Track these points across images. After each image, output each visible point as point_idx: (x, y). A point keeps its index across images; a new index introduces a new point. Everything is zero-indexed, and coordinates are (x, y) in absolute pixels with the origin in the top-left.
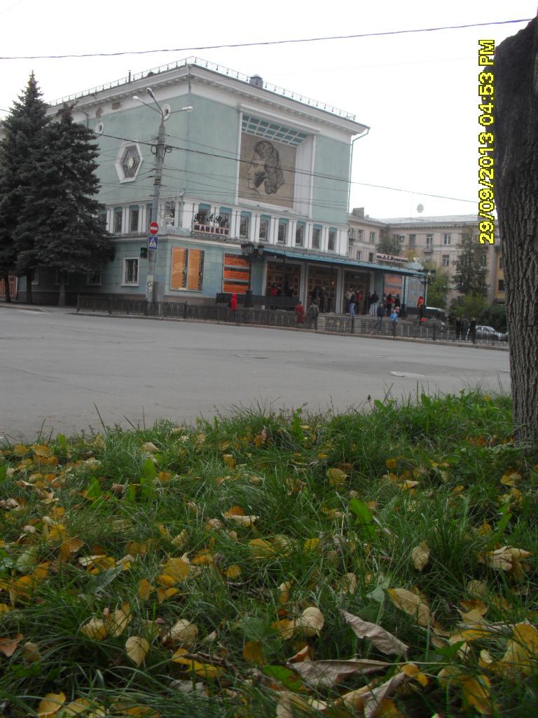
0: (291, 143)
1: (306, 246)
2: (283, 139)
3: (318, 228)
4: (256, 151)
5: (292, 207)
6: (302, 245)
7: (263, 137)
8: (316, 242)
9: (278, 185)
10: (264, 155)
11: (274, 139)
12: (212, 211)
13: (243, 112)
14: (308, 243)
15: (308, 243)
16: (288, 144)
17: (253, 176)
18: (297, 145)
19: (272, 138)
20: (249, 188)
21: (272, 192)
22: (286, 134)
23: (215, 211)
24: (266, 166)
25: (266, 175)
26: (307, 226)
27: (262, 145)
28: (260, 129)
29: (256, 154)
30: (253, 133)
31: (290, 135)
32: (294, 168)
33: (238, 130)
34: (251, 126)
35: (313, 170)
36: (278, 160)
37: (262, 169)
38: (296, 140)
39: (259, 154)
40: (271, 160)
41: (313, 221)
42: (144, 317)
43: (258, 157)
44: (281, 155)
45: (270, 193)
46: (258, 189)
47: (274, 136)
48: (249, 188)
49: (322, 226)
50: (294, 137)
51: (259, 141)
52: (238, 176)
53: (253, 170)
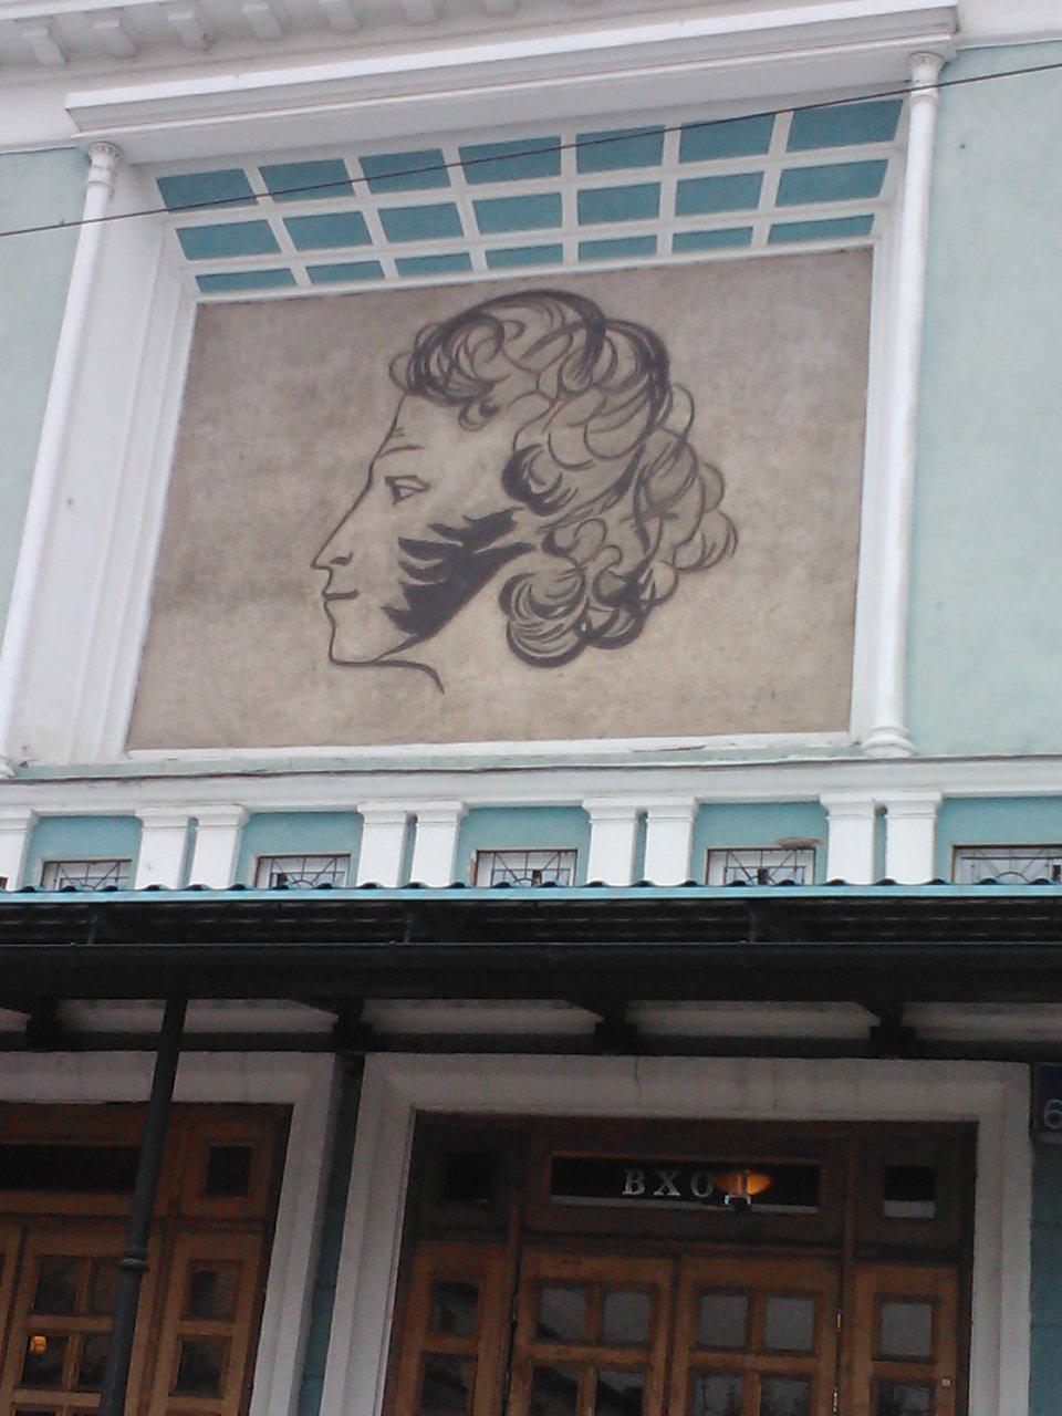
0: (779, 233)
2: (666, 225)
4: (421, 384)
7: (481, 272)
9: (661, 575)
10: (499, 395)
11: (589, 250)
13: (115, 149)
16: (759, 248)
18: (863, 224)
27: (478, 335)
29: (420, 402)
37: (488, 496)
39: (452, 401)
40: (591, 399)
43: (435, 424)
46: (427, 652)
47: (570, 233)
51: (446, 313)
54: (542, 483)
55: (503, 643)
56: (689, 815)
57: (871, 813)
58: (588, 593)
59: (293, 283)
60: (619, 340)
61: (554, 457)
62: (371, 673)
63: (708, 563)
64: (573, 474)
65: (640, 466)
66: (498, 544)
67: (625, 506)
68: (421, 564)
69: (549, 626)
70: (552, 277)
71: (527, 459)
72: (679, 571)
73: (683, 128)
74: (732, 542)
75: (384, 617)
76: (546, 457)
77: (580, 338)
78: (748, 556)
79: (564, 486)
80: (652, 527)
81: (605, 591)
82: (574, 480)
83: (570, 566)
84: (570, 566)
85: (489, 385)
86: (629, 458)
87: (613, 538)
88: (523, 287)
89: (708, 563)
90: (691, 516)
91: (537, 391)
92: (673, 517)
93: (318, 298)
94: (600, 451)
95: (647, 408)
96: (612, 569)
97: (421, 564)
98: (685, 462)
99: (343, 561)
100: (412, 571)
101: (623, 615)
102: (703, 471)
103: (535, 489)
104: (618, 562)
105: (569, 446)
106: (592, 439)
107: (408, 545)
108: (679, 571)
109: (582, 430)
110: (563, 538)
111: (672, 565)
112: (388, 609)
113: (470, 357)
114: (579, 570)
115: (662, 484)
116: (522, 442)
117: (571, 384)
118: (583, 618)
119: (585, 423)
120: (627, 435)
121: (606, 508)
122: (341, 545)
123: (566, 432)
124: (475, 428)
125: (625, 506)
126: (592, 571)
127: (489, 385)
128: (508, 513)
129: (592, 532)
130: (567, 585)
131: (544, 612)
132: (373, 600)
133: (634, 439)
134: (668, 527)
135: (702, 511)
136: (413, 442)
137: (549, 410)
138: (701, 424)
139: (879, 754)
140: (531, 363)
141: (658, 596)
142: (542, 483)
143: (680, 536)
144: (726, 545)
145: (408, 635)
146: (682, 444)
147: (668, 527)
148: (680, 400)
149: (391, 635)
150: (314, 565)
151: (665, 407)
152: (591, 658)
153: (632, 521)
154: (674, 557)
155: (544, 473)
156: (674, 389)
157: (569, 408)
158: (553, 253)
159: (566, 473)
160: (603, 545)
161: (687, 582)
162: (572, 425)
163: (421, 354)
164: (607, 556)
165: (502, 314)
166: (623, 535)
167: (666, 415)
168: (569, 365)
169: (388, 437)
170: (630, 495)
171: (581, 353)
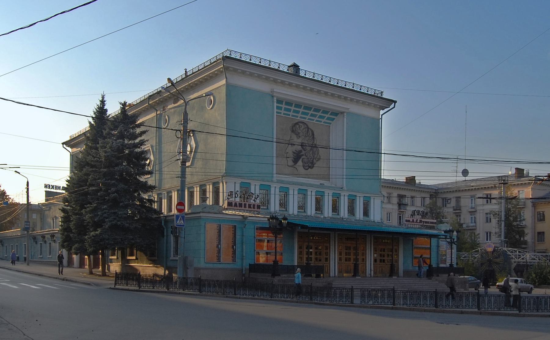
1: (342, 215)
2: (316, 119)
3: (353, 198)
4: (293, 131)
5: (327, 177)
6: (338, 214)
8: (352, 210)
9: (315, 161)
10: (301, 135)
11: (309, 119)
12: (253, 188)
14: (344, 212)
15: (344, 212)
16: (322, 123)
17: (291, 154)
19: (307, 119)
20: (288, 165)
21: (310, 167)
22: (319, 114)
23: (255, 189)
24: (302, 145)
25: (303, 152)
26: (342, 198)
27: (298, 126)
28: (295, 111)
29: (292, 133)
30: (289, 115)
31: (322, 115)
32: (330, 146)
33: (273, 113)
34: (286, 109)
35: (345, 145)
36: (313, 138)
37: (299, 148)
38: (328, 119)
39: (296, 134)
40: (308, 137)
42: (181, 291)
43: (294, 137)
44: (315, 134)
45: (307, 169)
46: (296, 166)
47: (308, 117)
48: (288, 165)
49: (356, 196)
50: (327, 116)
51: (295, 122)
52: (275, 155)
53: (290, 150)
59: (281, 114)
60: (310, 131)
62: (291, 168)
66: (301, 154)
68: (295, 155)
69: (306, 165)
70: (303, 120)
72: (316, 161)
73: (323, 110)
75: (292, 161)
77: (307, 130)
85: (299, 133)
88: (301, 121)
90: (317, 154)
93: (283, 116)
95: (312, 141)
97: (295, 155)
99: (288, 153)
100: (294, 155)
107: (293, 152)
108: (316, 161)
110: (307, 155)
112: (292, 160)
113: (297, 129)
118: (309, 165)
119: (308, 140)
122: (287, 151)
124: (298, 139)
127: (299, 133)
128: (302, 150)
131: (306, 163)
132: (291, 159)
135: (318, 154)
136: (293, 139)
145: (294, 164)
147: (315, 155)
148: (315, 140)
149: (293, 164)
150: (285, 153)
152: (310, 169)
158: (305, 118)
163: (292, 128)
165: (300, 124)
166: (312, 156)
169: (290, 138)
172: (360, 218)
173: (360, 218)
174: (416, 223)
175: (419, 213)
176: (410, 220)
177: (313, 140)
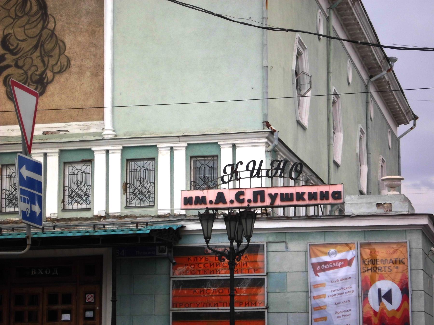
9: (49, 74)
40: (25, 19)
41: (115, 139)
54: (12, 45)
55: (5, 96)
56: (57, 154)
57: (105, 152)
58: (29, 80)
61: (16, 38)
63: (63, 71)
64: (22, 43)
65: (41, 40)
67: (37, 53)
71: (8, 37)
72: (54, 73)
74: (69, 64)
76: (13, 37)
78: (74, 69)
79: (19, 47)
80: (46, 59)
81: (34, 80)
82: (23, 45)
83: (23, 72)
84: (23, 72)
86: (38, 38)
87: (35, 63)
89: (63, 71)
90: (57, 56)
91: (9, 16)
92: (52, 56)
94: (29, 35)
95: (42, 22)
96: (36, 73)
98: (54, 38)
101: (40, 87)
102: (59, 42)
103: (11, 48)
104: (37, 70)
105: (20, 33)
106: (26, 31)
108: (54, 73)
109: (23, 29)
110: (20, 63)
111: (52, 71)
114: (26, 73)
115: (48, 46)
116: (6, 32)
117: (20, 15)
119: (24, 26)
120: (36, 31)
121: (31, 54)
123: (19, 29)
125: (37, 53)
126: (30, 73)
128: (4, 55)
129: (29, 60)
130: (23, 77)
133: (38, 32)
134: (50, 59)
137: (12, 23)
138: (58, 27)
139: (106, 137)
140: (7, 7)
141: (49, 81)
142: (12, 45)
143: (54, 62)
144: (67, 65)
146: (53, 34)
148: (51, 19)
151: (47, 21)
153: (40, 58)
154: (53, 68)
155: (13, 42)
156: (50, 16)
157: (19, 22)
159: (19, 42)
160: (32, 65)
161: (57, 77)
162: (20, 27)
164: (33, 69)
166: (38, 62)
167: (47, 25)
168: (18, 7)
170: (39, 49)
171: (21, 4)
172: (172, 210)
173: (172, 210)
174: (236, 204)
175: (259, 170)
176: (204, 198)
177: (44, 23)
